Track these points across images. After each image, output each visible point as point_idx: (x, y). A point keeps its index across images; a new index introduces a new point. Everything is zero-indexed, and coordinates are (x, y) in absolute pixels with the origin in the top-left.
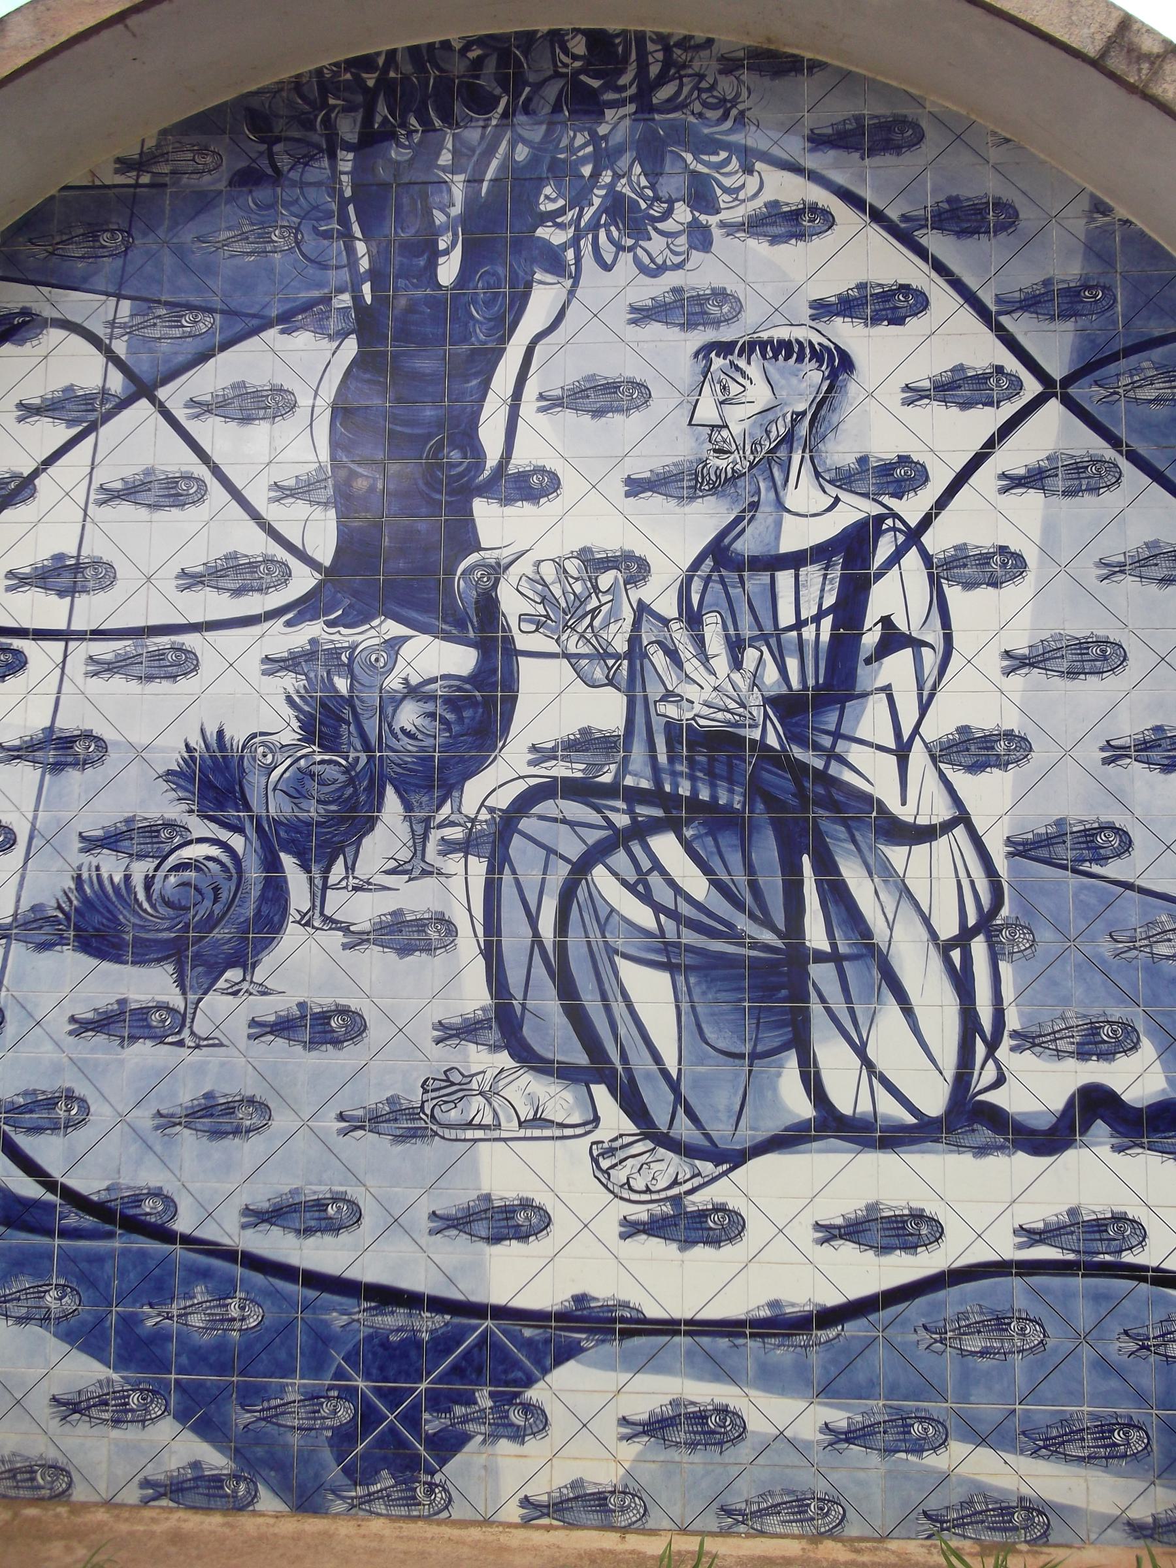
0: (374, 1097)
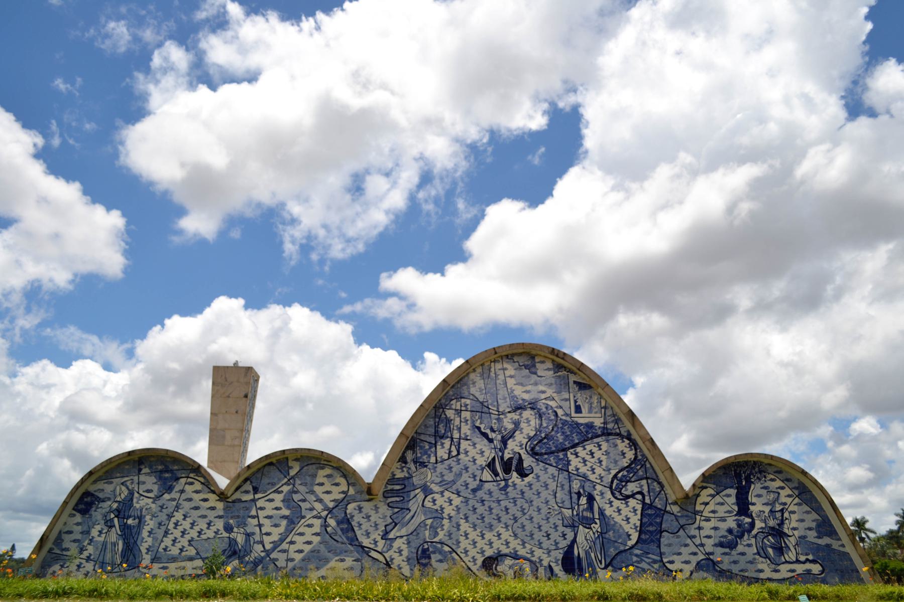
0: (748, 560)
